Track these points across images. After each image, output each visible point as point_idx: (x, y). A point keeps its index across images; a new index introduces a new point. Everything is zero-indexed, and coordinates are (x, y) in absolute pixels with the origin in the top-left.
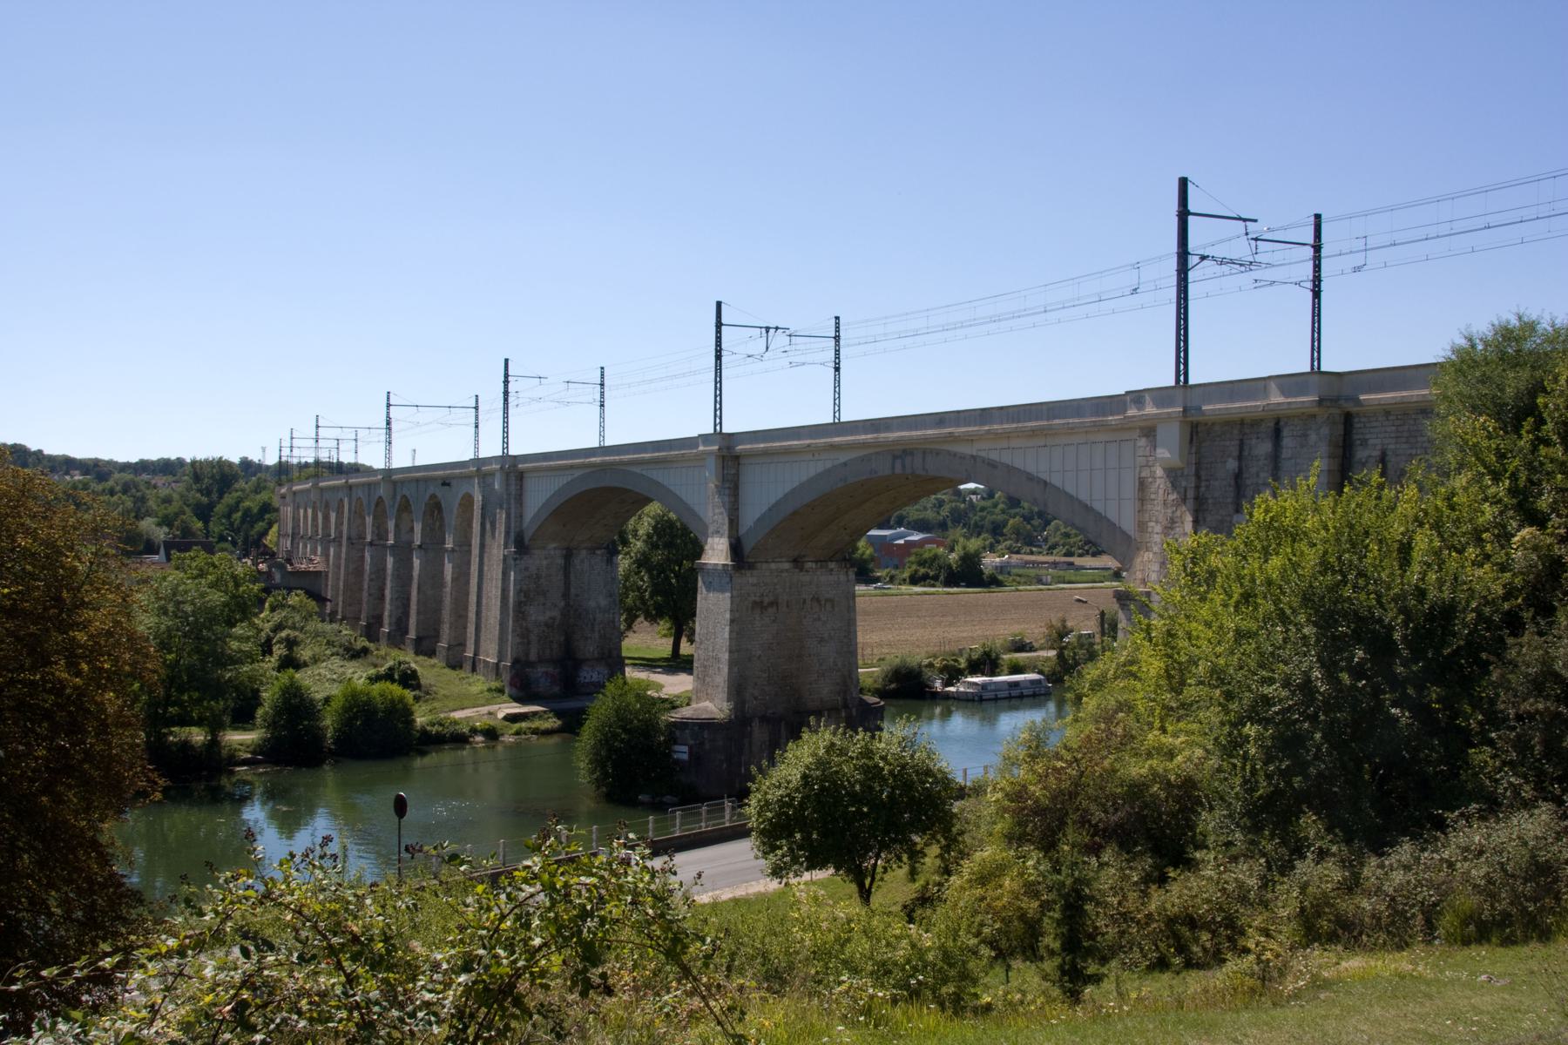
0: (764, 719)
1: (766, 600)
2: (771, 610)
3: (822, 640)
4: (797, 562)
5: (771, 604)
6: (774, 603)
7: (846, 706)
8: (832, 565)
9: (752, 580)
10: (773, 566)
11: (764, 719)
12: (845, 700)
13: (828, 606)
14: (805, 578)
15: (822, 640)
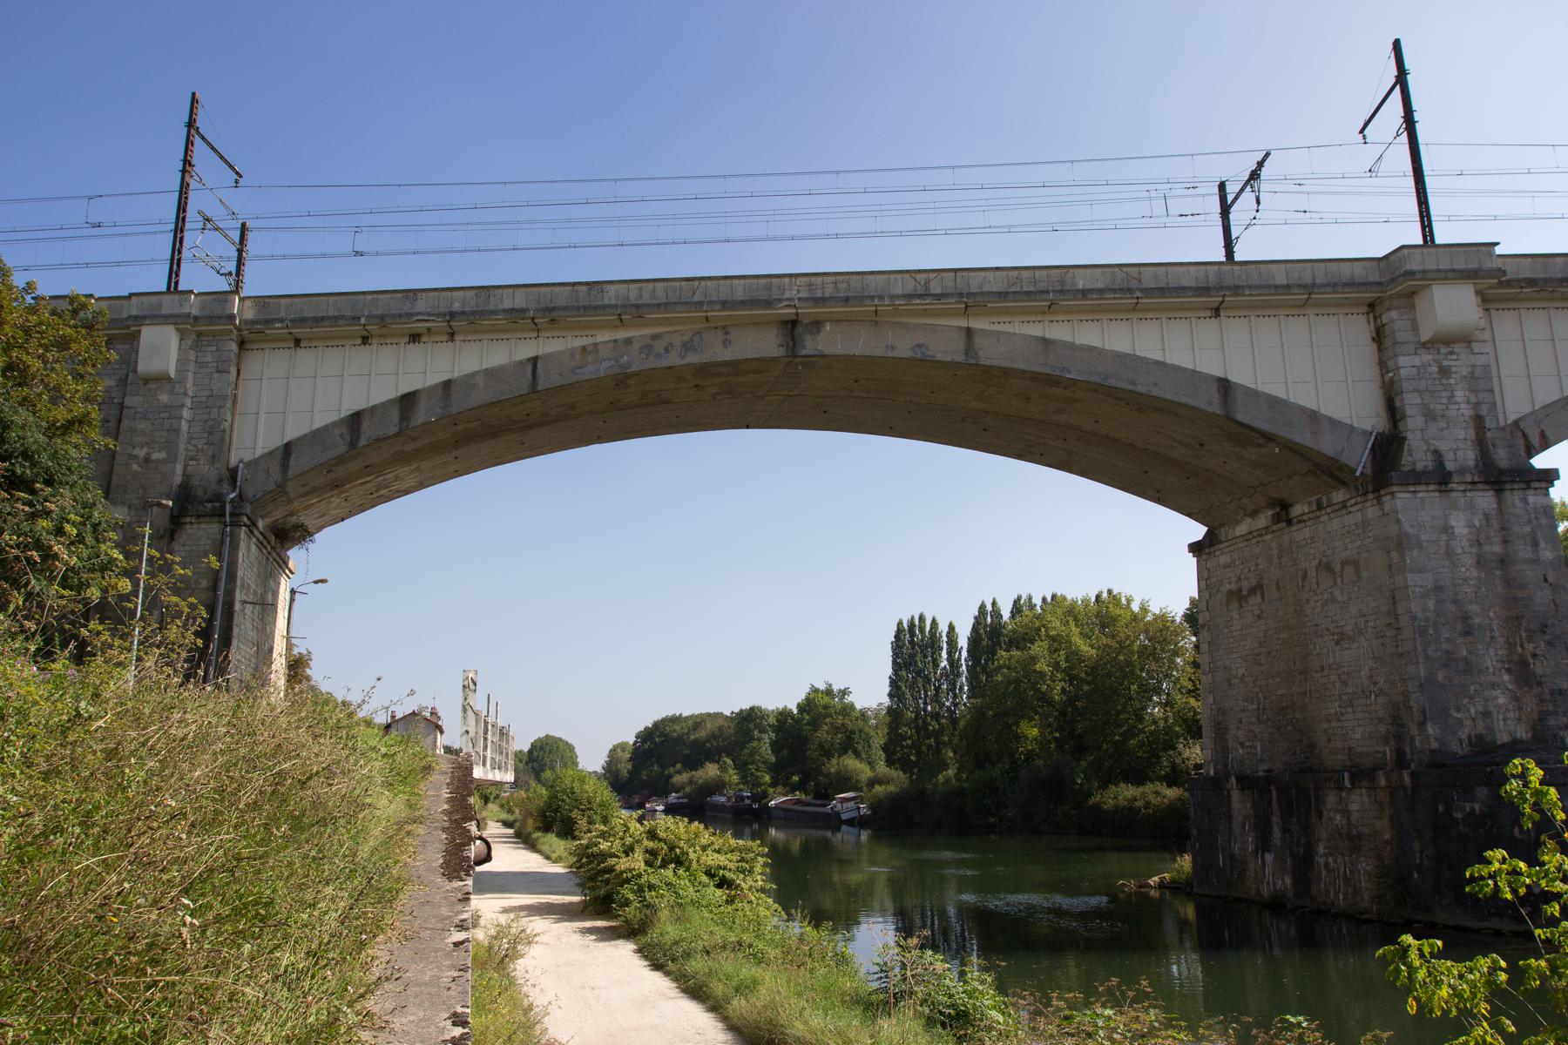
0: (1245, 782)
1: (1245, 585)
2: (1255, 600)
3: (1342, 638)
4: (1282, 512)
5: (1253, 591)
6: (1258, 589)
7: (1401, 762)
8: (1339, 496)
9: (1224, 559)
10: (1241, 529)
11: (1245, 782)
12: (1400, 753)
13: (1349, 572)
14: (1301, 534)
15: (1342, 638)
